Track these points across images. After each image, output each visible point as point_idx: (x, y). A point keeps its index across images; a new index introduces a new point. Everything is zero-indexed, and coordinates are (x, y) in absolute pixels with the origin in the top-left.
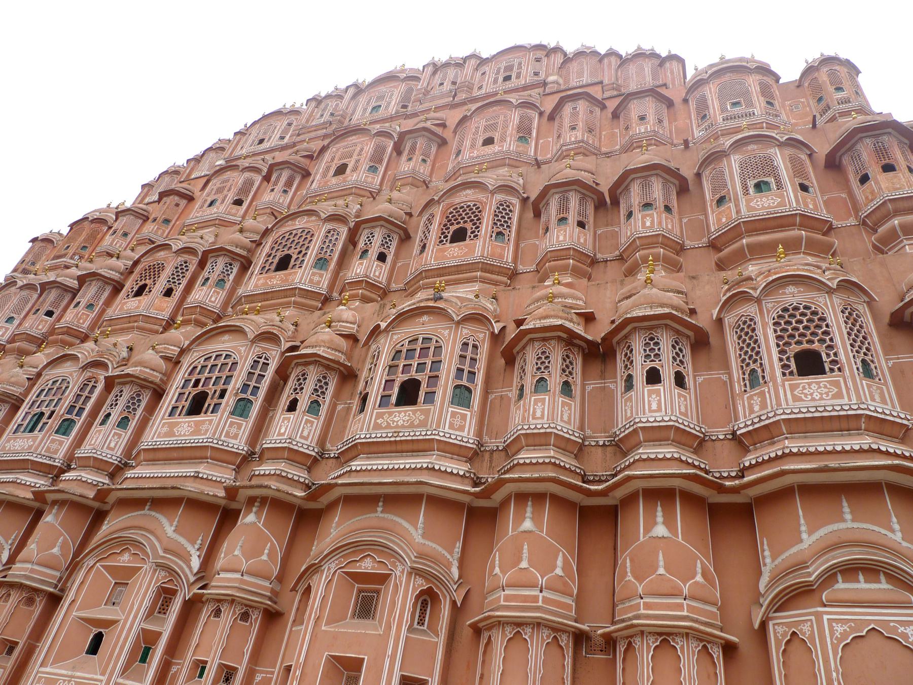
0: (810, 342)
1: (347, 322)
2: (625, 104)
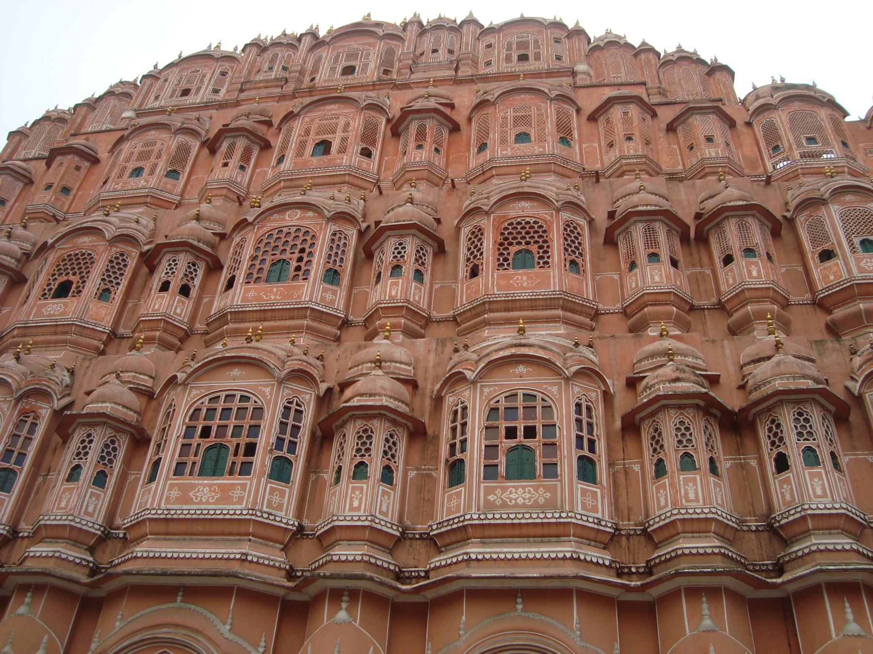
1: (401, 363)
2: (684, 117)
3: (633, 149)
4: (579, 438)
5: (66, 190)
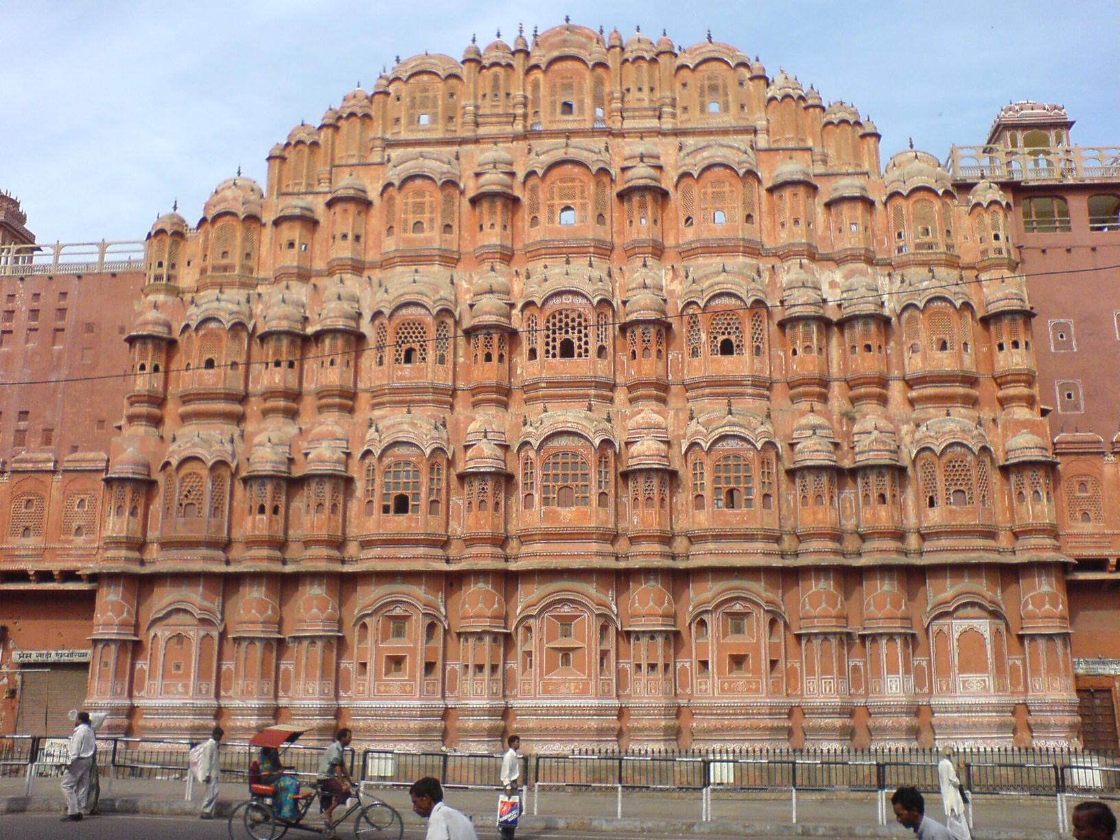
3: (799, 236)
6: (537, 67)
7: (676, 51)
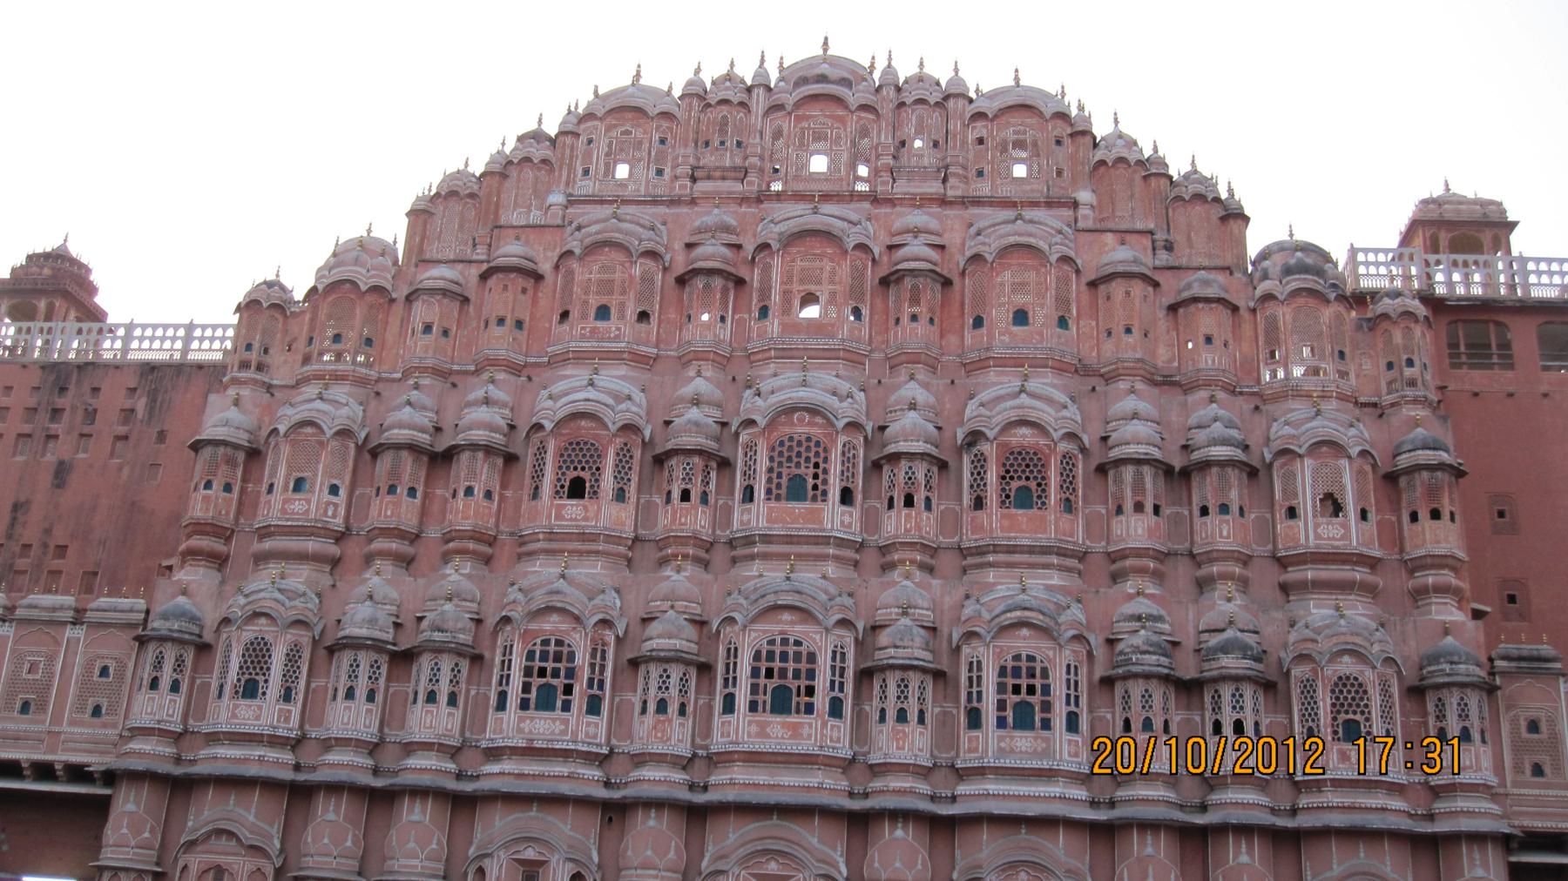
0: (1355, 713)
3: (1130, 348)
4: (1068, 696)
5: (519, 324)
6: (779, 107)
7: (973, 95)
